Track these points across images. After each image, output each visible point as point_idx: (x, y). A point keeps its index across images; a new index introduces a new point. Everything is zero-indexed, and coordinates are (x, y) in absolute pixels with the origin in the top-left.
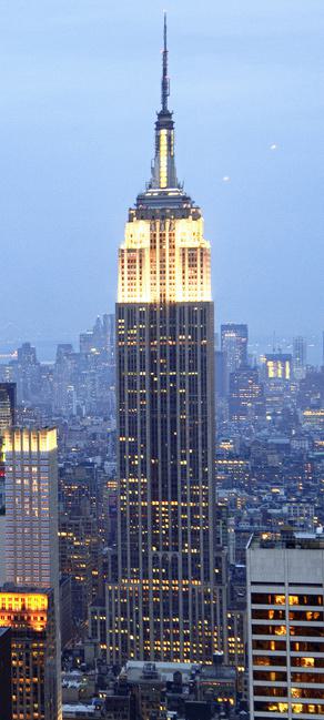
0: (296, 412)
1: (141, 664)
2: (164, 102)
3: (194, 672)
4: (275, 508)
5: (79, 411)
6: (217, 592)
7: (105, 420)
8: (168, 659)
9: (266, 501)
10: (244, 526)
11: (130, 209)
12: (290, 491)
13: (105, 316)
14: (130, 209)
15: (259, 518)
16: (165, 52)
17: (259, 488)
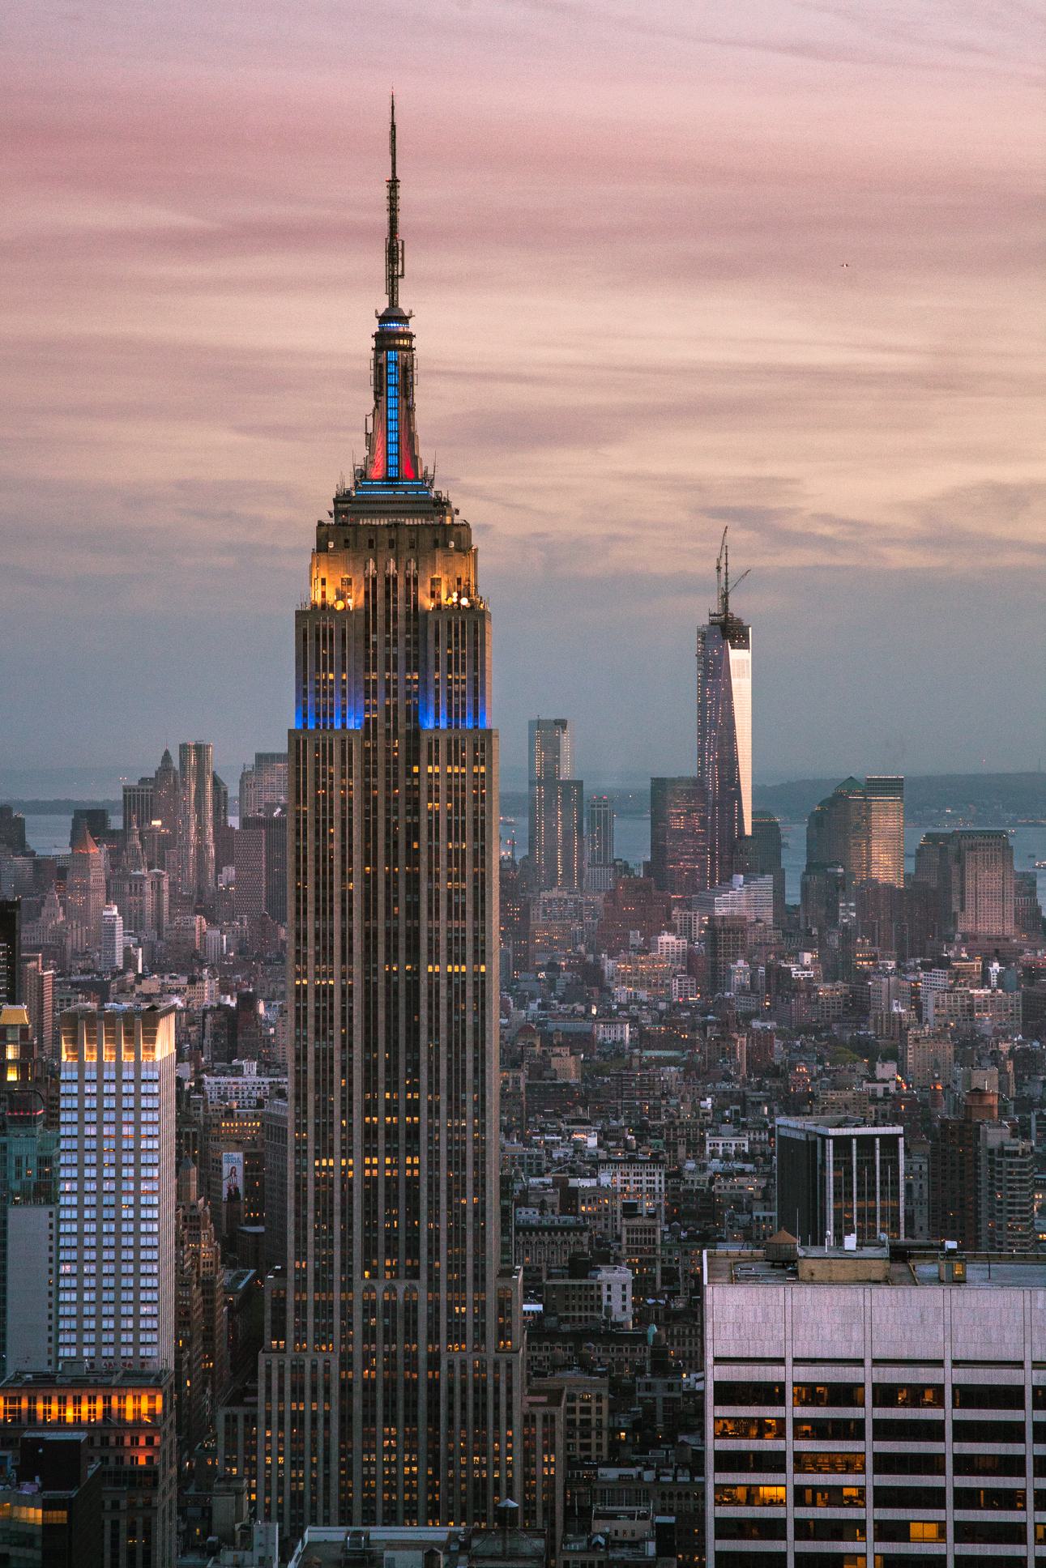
0: (597, 960)
1: (337, 1534)
2: (392, 292)
3: (454, 1547)
4: (583, 1176)
5: (130, 961)
6: (503, 1365)
7: (192, 981)
8: (391, 1519)
9: (559, 1162)
10: (528, 1215)
11: (321, 524)
12: (604, 1136)
13: (184, 748)
14: (321, 524)
15: (553, 1197)
16: (393, 184)
17: (543, 1131)
